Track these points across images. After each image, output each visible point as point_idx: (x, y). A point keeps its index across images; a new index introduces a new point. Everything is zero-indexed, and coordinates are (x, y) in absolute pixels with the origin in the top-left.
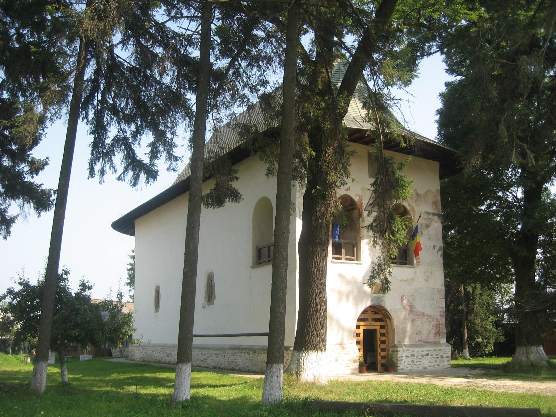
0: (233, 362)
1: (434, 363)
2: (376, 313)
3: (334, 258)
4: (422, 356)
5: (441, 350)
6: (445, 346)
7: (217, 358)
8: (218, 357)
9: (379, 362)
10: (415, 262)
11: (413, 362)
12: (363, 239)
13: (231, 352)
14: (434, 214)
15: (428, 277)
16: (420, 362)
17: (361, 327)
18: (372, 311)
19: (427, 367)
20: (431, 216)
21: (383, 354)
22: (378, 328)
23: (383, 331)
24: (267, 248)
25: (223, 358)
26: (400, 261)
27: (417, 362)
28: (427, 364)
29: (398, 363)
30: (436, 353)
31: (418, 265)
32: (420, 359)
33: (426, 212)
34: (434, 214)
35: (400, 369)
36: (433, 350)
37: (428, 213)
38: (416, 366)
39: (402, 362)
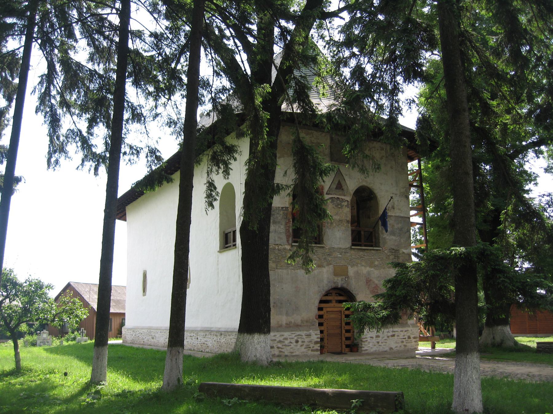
0: (204, 343)
1: (400, 344)
2: (340, 295)
4: (388, 337)
5: (408, 330)
6: (412, 327)
7: (191, 340)
8: (192, 339)
11: (378, 342)
13: (202, 334)
16: (386, 342)
17: (324, 309)
18: (336, 293)
19: (393, 347)
24: (232, 233)
25: (196, 340)
26: (366, 243)
27: (382, 343)
28: (393, 345)
29: (362, 344)
30: (402, 334)
32: (385, 340)
35: (364, 350)
36: (399, 331)
38: (381, 347)
39: (366, 343)
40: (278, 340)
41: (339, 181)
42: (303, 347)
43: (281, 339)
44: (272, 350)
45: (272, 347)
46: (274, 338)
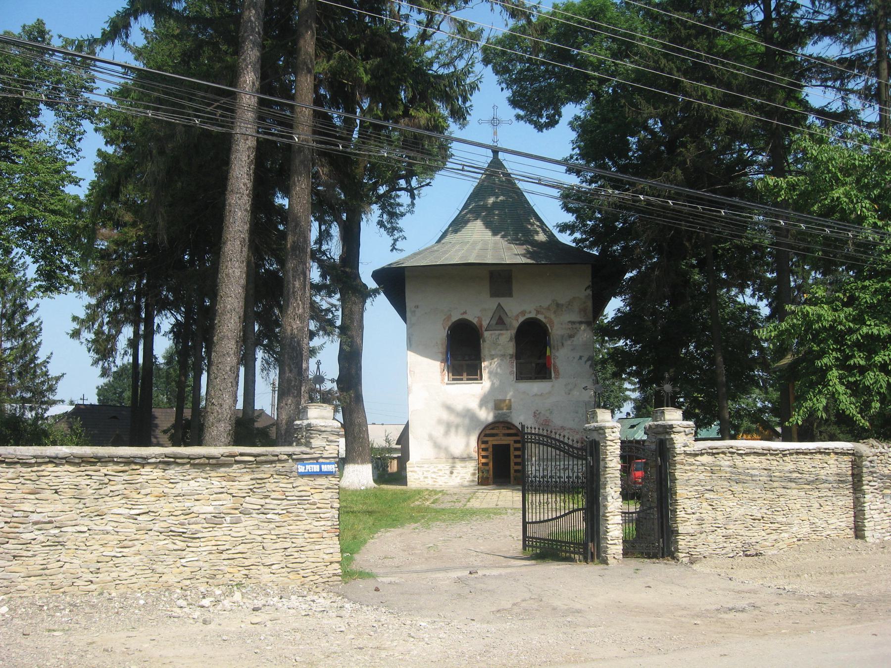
2: (509, 428)
3: (454, 380)
9: (512, 475)
10: (553, 375)
12: (484, 361)
14: (581, 323)
15: (571, 390)
20: (577, 325)
21: (519, 467)
22: (512, 442)
23: (519, 445)
31: (556, 378)
33: (569, 322)
34: (581, 323)
37: (573, 323)
40: (432, 471)
41: (500, 316)
42: (459, 478)
43: (435, 470)
44: (426, 480)
45: (426, 477)
46: (427, 469)
